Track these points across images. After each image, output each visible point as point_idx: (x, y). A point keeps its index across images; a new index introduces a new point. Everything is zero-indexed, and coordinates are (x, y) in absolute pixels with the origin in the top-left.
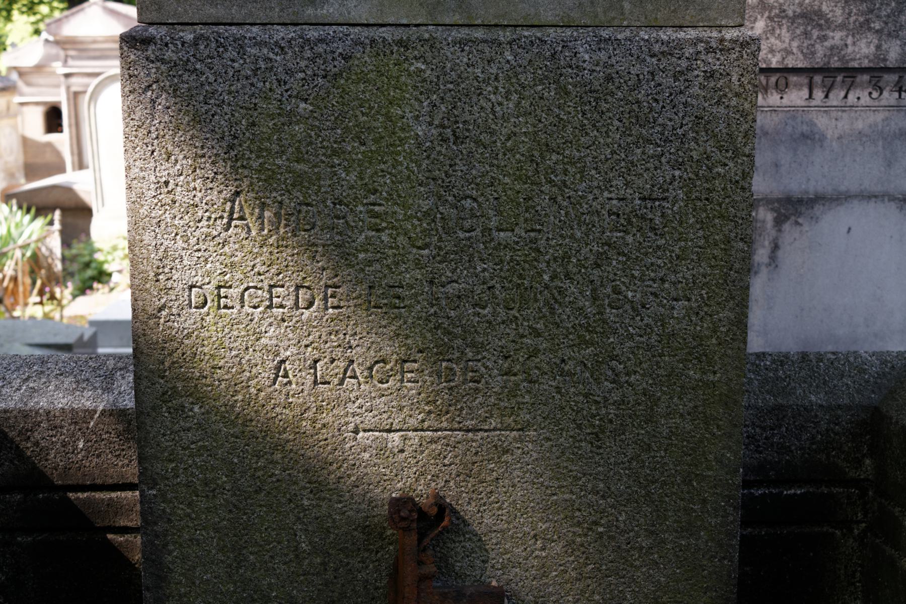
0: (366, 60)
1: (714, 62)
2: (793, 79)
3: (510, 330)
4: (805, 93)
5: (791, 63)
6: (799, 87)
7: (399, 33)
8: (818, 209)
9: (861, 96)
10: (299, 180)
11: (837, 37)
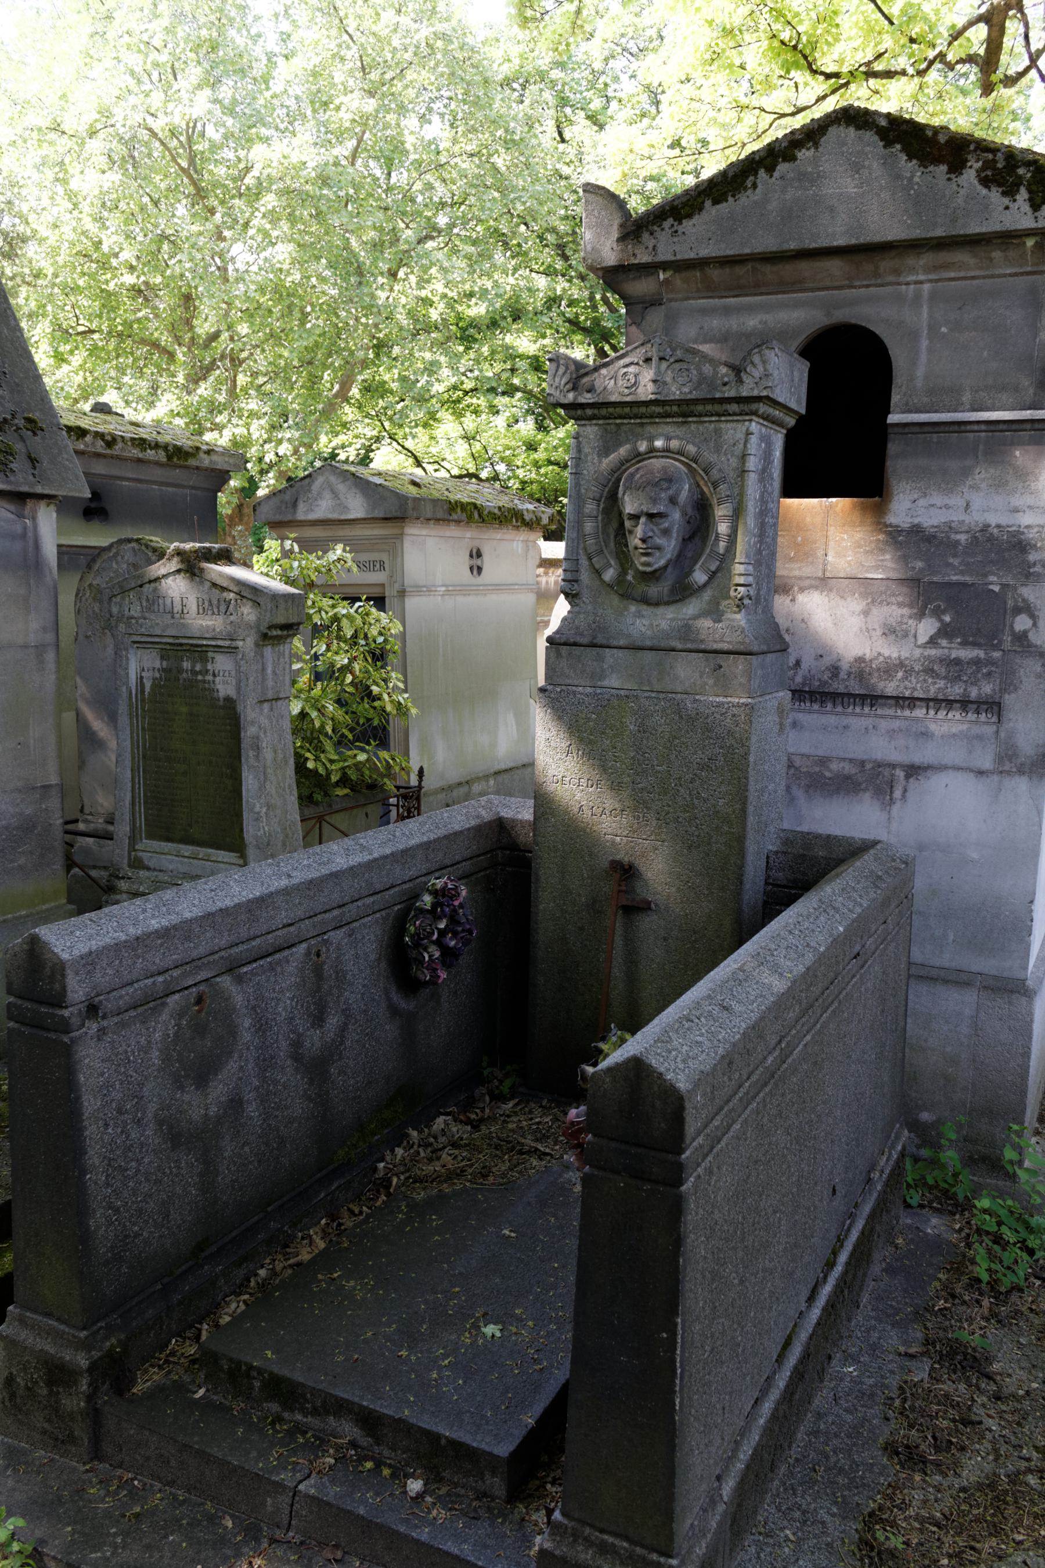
0: (615, 702)
1: (735, 710)
2: (918, 703)
3: (660, 804)
4: (924, 711)
5: (916, 695)
6: (921, 707)
7: (627, 693)
8: (929, 773)
9: (956, 714)
10: (590, 742)
11: (941, 683)
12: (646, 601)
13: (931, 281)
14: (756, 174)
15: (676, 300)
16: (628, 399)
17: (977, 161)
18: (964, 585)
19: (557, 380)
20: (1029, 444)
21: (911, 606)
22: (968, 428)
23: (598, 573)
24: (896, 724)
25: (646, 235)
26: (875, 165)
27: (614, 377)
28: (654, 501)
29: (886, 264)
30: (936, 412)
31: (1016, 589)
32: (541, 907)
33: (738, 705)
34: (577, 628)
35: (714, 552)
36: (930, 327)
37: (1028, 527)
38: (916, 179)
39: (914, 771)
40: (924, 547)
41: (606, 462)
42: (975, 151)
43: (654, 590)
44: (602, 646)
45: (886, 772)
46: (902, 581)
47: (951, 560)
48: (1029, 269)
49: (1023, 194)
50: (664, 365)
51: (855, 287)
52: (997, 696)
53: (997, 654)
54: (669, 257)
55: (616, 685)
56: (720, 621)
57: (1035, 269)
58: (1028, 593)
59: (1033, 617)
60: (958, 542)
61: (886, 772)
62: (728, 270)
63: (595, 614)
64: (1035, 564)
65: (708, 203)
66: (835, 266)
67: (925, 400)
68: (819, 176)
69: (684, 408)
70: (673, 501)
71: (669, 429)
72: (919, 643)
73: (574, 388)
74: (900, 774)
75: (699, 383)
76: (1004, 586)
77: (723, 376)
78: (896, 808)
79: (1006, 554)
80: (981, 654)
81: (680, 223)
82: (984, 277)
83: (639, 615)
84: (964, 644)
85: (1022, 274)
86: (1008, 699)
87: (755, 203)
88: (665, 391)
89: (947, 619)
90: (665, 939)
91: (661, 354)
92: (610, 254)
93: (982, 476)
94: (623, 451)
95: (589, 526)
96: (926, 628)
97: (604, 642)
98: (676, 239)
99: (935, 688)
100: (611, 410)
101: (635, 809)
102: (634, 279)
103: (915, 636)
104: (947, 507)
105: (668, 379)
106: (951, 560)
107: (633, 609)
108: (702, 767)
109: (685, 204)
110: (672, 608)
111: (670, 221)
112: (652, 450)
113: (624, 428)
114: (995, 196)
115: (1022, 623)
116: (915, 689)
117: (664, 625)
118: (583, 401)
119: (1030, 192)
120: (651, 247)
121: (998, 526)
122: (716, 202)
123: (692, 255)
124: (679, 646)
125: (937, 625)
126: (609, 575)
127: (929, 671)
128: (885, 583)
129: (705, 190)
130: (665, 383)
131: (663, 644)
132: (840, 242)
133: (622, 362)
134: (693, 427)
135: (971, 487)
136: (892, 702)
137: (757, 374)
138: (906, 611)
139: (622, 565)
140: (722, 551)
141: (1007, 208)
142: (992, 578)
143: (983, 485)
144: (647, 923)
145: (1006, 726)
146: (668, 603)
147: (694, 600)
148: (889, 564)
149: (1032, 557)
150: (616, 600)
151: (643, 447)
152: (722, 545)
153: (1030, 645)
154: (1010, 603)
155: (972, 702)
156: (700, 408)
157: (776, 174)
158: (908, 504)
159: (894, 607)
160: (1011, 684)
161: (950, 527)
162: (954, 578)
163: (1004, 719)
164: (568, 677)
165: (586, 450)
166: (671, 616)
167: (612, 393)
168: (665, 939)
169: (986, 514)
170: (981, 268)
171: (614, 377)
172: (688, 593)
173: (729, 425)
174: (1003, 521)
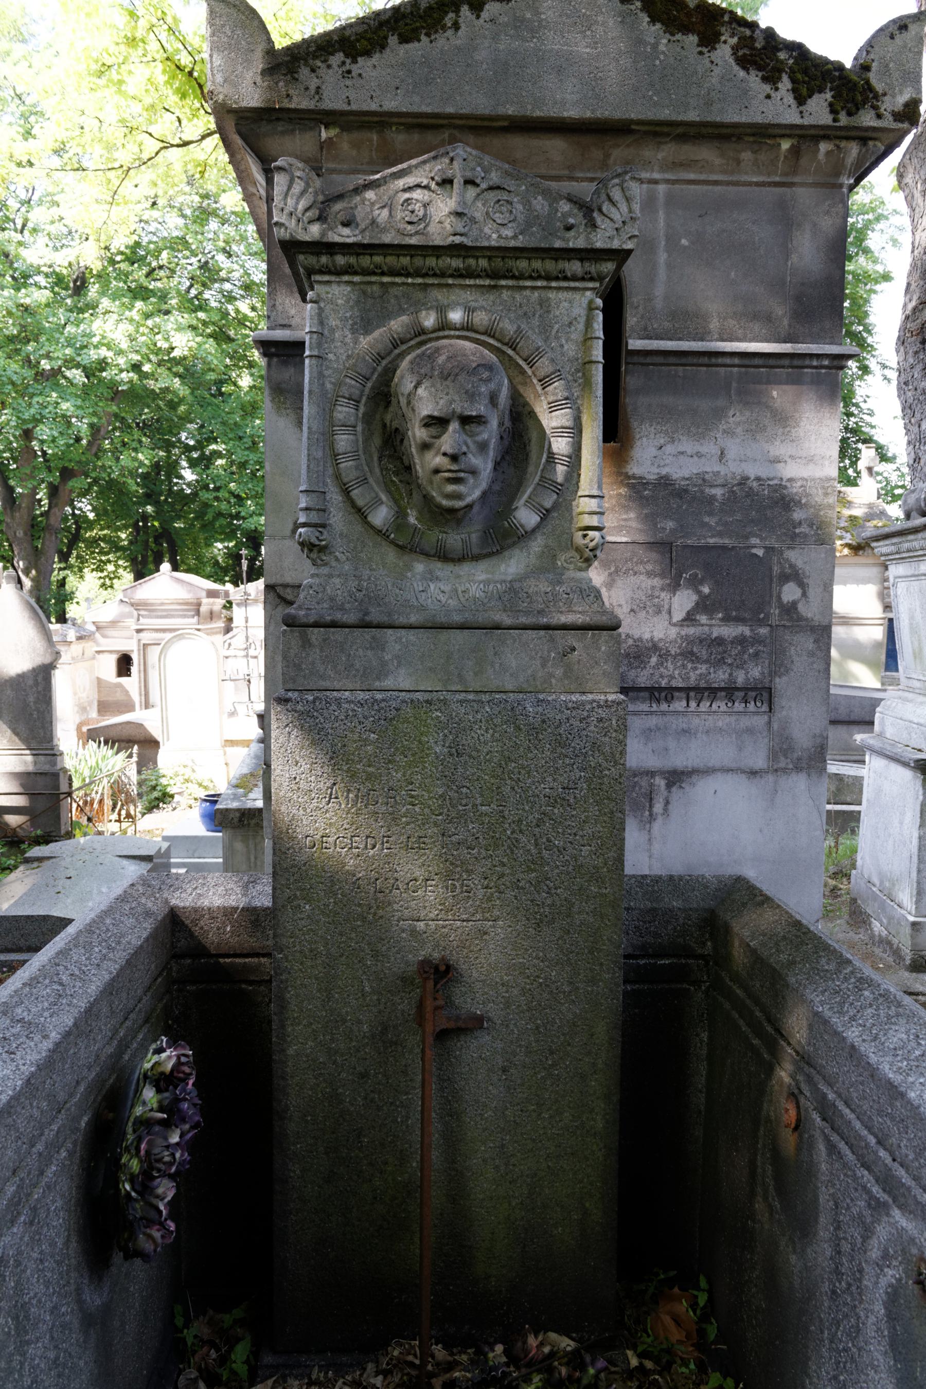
0: (408, 711)
1: (602, 713)
2: (676, 694)
3: (488, 863)
4: (684, 703)
5: (674, 684)
6: (680, 699)
7: (427, 696)
8: (695, 778)
9: (720, 705)
10: (369, 777)
11: (702, 669)
12: (444, 556)
13: (667, 181)
14: (457, 11)
15: (340, 172)
16: (413, 241)
17: (732, 36)
18: (724, 548)
19: (290, 202)
20: (787, 383)
21: (662, 575)
22: (720, 360)
23: (361, 513)
24: (653, 721)
25: (304, 72)
26: (611, 22)
27: (389, 205)
28: (472, 396)
29: (619, 152)
30: (680, 339)
31: (781, 553)
32: (291, 1052)
33: (607, 705)
35: (547, 483)
36: (668, 238)
37: (790, 480)
38: (662, 48)
39: (676, 778)
40: (674, 503)
41: (365, 342)
42: (730, 23)
43: (454, 539)
44: (379, 626)
45: (644, 782)
46: (652, 545)
47: (707, 519)
48: (777, 179)
49: (785, 84)
50: (471, 192)
51: (576, 179)
52: (767, 680)
53: (763, 631)
54: (339, 105)
55: (406, 685)
56: (560, 583)
57: (784, 180)
58: (795, 556)
59: (802, 585)
60: (713, 497)
61: (644, 782)
62: (416, 137)
63: (358, 577)
64: (800, 523)
65: (393, 40)
66: (556, 147)
67: (667, 324)
68: (540, 26)
69: (498, 263)
70: (493, 399)
71: (468, 296)
72: (674, 620)
73: (321, 218)
74: (660, 782)
75: (528, 224)
76: (769, 550)
77: (565, 216)
78: (657, 826)
79: (768, 513)
80: (747, 631)
81: (355, 61)
82: (728, 183)
83: (431, 577)
84: (727, 619)
85: (770, 184)
86: (780, 683)
87: (459, 49)
88: (475, 233)
89: (706, 590)
90: (504, 1070)
91: (469, 174)
92: (250, 94)
93: (738, 418)
94: (398, 324)
95: (343, 441)
96: (683, 601)
97: (385, 619)
98: (348, 82)
99: (695, 674)
100: (378, 259)
101: (449, 875)
102: (283, 133)
103: (669, 612)
104: (699, 455)
105: (478, 215)
106: (707, 519)
107: (420, 567)
108: (553, 801)
109: (361, 36)
110: (483, 565)
111: (339, 57)
112: (444, 326)
113: (394, 291)
114: (754, 79)
115: (790, 592)
116: (672, 677)
117: (475, 591)
118: (338, 239)
119: (793, 81)
120: (313, 88)
121: (758, 479)
122: (404, 39)
123: (374, 107)
124: (508, 621)
125: (695, 598)
126: (381, 516)
127: (688, 655)
128: (630, 547)
129: (387, 22)
130: (473, 220)
131: (481, 618)
132: (572, 113)
133: (401, 183)
134: (505, 294)
135: (724, 431)
136: (646, 694)
137: (616, 216)
138: (657, 582)
139: (396, 501)
140: (560, 478)
141: (768, 97)
142: (754, 541)
143: (739, 430)
144: (476, 1051)
145: (780, 714)
146: (476, 558)
147: (516, 552)
148: (634, 524)
149: (797, 515)
150: (391, 555)
151: (429, 321)
152: (561, 470)
153: (800, 618)
154: (776, 569)
155: (738, 689)
156: (523, 264)
157: (485, 15)
158: (653, 451)
159: (642, 577)
160: (782, 665)
161: (703, 480)
162: (712, 541)
163: (776, 707)
164: (322, 677)
165: (333, 322)
166: (483, 577)
167: (384, 230)
168: (504, 1070)
169: (743, 465)
170: (724, 172)
171: (389, 205)
172: (510, 541)
173: (562, 295)
174: (764, 473)
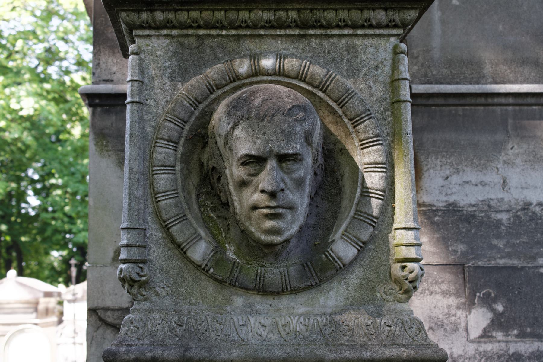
12: (263, 290)
18: (513, 268)
21: (457, 295)
22: (496, 100)
23: (180, 249)
30: (457, 83)
34: (152, 334)
35: (362, 216)
40: (463, 227)
41: (182, 89)
43: (273, 273)
47: (495, 242)
56: (380, 315)
60: (499, 222)
67: (445, 71)
70: (308, 138)
71: (279, 45)
72: (472, 337)
84: (522, 336)
89: (500, 308)
93: (516, 150)
94: (214, 72)
95: (163, 180)
103: (467, 330)
104: (483, 184)
106: (495, 242)
107: (239, 301)
110: (302, 298)
112: (257, 72)
113: (209, 42)
125: (490, 315)
126: (200, 251)
134: (314, 42)
135: (505, 162)
138: (452, 301)
139: (214, 236)
140: (375, 212)
143: (518, 161)
146: (295, 291)
150: (210, 289)
151: (243, 67)
152: (376, 204)
158: (440, 181)
161: (488, 206)
166: (302, 310)
169: (525, 192)
172: (328, 274)
173: (368, 42)
